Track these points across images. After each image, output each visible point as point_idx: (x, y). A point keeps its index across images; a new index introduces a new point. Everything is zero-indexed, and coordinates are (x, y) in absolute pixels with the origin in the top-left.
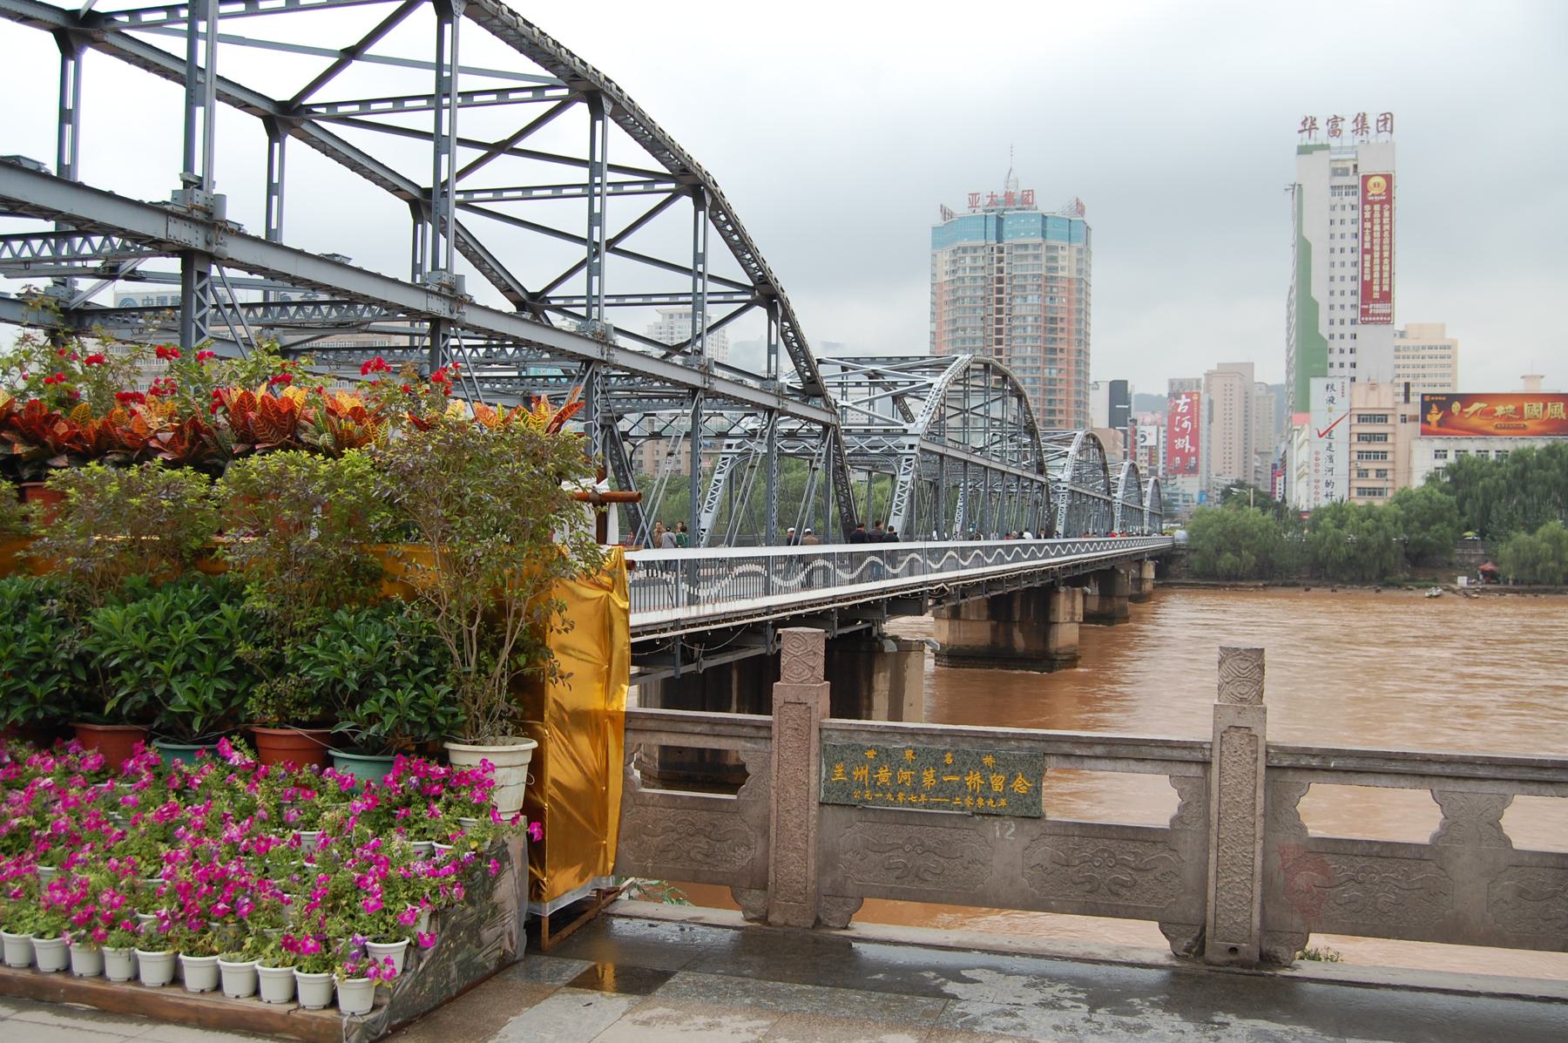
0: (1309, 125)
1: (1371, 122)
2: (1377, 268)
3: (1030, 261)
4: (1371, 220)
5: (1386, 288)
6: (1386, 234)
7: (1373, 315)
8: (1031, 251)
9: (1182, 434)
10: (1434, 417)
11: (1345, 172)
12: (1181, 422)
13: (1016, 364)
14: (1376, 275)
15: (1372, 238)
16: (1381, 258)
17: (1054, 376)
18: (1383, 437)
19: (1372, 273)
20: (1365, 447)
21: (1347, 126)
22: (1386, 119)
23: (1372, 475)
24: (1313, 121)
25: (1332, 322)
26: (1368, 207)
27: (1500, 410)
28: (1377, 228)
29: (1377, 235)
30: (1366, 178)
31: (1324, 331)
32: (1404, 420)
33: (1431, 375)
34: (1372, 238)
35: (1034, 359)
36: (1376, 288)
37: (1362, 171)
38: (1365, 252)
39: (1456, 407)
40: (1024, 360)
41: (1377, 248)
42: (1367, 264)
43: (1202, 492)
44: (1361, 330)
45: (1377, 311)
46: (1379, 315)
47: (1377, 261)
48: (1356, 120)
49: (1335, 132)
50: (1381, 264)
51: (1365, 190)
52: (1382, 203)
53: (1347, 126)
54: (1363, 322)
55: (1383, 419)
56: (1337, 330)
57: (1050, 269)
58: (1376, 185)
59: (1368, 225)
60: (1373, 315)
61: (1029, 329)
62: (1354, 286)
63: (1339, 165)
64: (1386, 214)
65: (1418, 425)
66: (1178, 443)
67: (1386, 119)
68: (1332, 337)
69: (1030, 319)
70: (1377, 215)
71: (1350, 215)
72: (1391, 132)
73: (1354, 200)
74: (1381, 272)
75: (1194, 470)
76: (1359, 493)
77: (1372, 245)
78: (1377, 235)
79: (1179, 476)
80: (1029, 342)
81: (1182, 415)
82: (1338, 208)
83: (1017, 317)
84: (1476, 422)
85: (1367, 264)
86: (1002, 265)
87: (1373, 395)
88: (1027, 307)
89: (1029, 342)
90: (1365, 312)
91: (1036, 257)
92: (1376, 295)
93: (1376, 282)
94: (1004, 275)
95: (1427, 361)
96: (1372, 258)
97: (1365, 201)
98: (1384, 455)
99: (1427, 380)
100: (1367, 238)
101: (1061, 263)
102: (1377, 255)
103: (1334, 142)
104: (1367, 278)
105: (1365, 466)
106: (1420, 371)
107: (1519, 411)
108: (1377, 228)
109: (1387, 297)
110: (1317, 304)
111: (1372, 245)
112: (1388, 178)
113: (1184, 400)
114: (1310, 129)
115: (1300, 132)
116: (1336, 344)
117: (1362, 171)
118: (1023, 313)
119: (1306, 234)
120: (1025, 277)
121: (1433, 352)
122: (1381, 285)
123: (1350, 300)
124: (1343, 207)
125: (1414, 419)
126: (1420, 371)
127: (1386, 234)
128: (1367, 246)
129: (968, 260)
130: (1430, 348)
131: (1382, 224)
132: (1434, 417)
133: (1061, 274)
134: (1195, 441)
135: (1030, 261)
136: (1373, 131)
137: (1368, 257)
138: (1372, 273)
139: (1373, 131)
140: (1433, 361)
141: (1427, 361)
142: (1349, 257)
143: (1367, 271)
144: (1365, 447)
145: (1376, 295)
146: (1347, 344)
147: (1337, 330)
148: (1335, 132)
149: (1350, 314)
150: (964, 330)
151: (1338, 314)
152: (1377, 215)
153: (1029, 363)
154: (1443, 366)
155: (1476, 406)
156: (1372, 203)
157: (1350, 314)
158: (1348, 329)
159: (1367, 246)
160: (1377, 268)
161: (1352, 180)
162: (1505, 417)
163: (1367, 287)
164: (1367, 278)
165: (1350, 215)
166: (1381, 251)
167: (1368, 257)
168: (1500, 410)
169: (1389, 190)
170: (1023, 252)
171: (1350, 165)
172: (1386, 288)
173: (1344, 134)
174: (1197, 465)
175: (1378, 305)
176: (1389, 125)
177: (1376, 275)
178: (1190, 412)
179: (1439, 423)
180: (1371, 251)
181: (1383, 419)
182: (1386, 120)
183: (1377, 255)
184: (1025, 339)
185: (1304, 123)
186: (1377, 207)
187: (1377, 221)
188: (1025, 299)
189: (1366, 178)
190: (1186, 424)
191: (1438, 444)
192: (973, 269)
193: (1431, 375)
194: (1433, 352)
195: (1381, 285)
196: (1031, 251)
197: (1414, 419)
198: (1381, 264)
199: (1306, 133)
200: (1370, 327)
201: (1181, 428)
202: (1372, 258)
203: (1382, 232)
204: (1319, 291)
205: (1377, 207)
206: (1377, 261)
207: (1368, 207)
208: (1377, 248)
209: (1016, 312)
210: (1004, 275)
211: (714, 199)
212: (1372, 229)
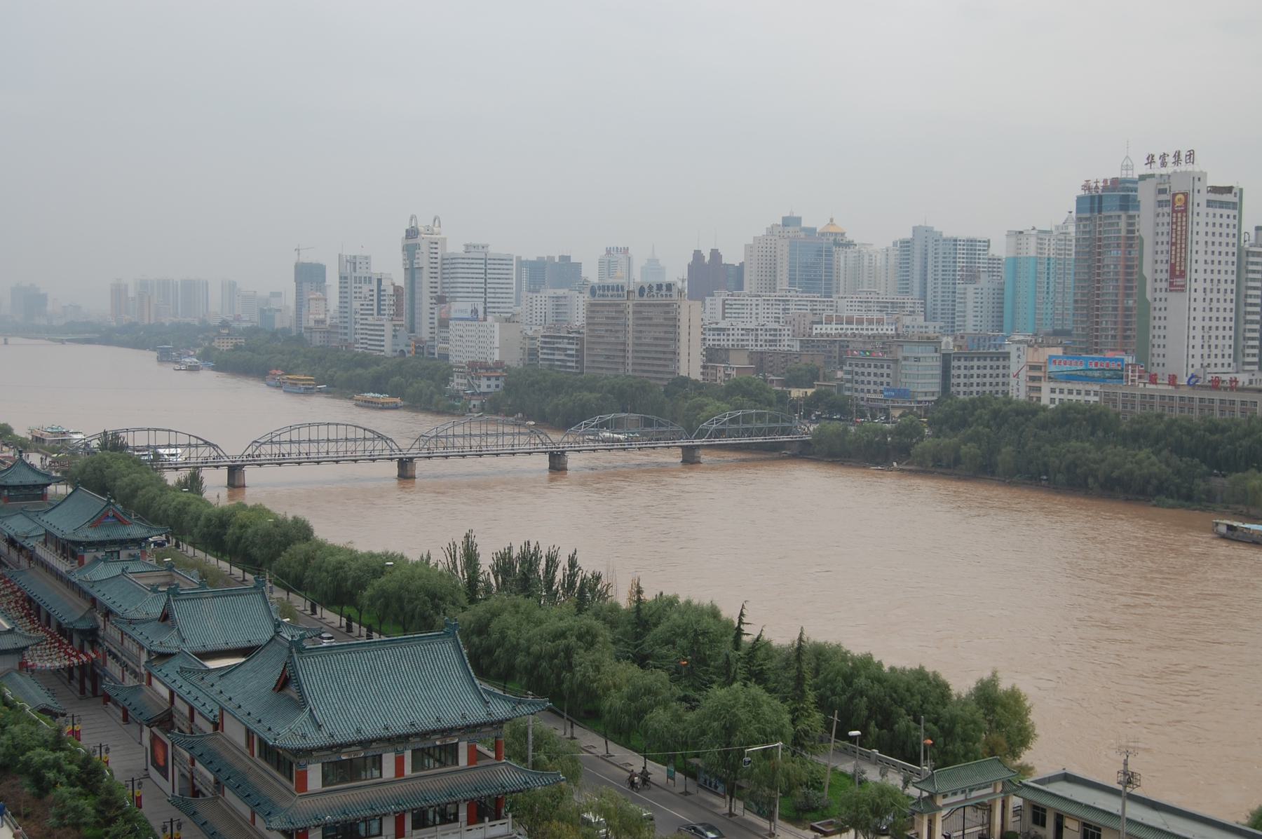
1: (1183, 157)
2: (1178, 255)
4: (1176, 223)
5: (1183, 268)
6: (1184, 232)
7: (1176, 286)
14: (1178, 260)
15: (1176, 234)
16: (1181, 248)
19: (1176, 258)
21: (1170, 160)
24: (1153, 156)
26: (1174, 215)
28: (1179, 228)
29: (1179, 233)
30: (1175, 195)
31: (1149, 296)
34: (1176, 234)
36: (1178, 268)
38: (1173, 244)
41: (1179, 242)
42: (1173, 253)
45: (1178, 284)
46: (1178, 286)
47: (1178, 250)
48: (1175, 155)
50: (1181, 252)
51: (1174, 204)
52: (1182, 211)
53: (1170, 160)
54: (1171, 291)
56: (1158, 295)
58: (1180, 200)
59: (1174, 227)
60: (1176, 286)
62: (1166, 267)
64: (1184, 219)
69: (1112, 267)
70: (1179, 220)
71: (1167, 219)
72: (1193, 163)
73: (1167, 210)
74: (1181, 257)
77: (1176, 240)
78: (1179, 233)
85: (1173, 253)
88: (1113, 256)
90: (1171, 284)
92: (1178, 273)
93: (1178, 264)
96: (1176, 248)
97: (1174, 211)
100: (1174, 235)
102: (1178, 246)
104: (1173, 261)
108: (1179, 228)
109: (1183, 274)
110: (1146, 279)
111: (1176, 240)
114: (1151, 162)
122: (1180, 266)
123: (1165, 276)
124: (1163, 215)
127: (1184, 232)
128: (1174, 240)
131: (1182, 226)
137: (1174, 248)
138: (1176, 258)
142: (1165, 247)
143: (1173, 257)
145: (1178, 273)
147: (1158, 295)
148: (1164, 164)
149: (1165, 285)
151: (1158, 285)
152: (1179, 220)
156: (1177, 212)
158: (1163, 295)
159: (1174, 240)
160: (1178, 255)
163: (1173, 267)
164: (1173, 261)
166: (1181, 243)
167: (1174, 248)
169: (1186, 203)
172: (1183, 268)
173: (1168, 165)
175: (1178, 280)
177: (1178, 260)
182: (1191, 154)
183: (1178, 246)
185: (1148, 159)
186: (1179, 215)
187: (1179, 224)
189: (1175, 195)
195: (1180, 266)
198: (1181, 252)
200: (1174, 294)
202: (1176, 248)
203: (1182, 231)
205: (1179, 215)
206: (1178, 250)
207: (1174, 215)
208: (1179, 242)
212: (1176, 229)
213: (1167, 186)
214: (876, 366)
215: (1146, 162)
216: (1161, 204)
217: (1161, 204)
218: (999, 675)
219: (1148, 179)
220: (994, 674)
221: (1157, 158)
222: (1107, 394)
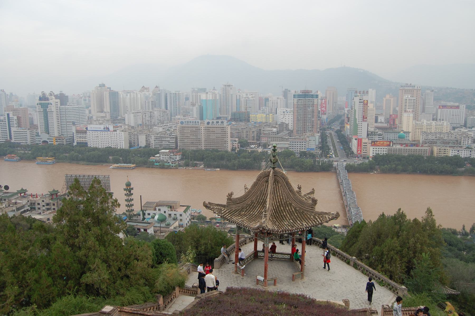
1: (365, 92)
3: (310, 102)
8: (310, 100)
9: (323, 107)
10: (373, 144)
11: (361, 100)
12: (323, 105)
13: (308, 118)
18: (366, 146)
20: (364, 147)
27: (381, 143)
30: (364, 101)
31: (357, 122)
32: (369, 143)
35: (311, 118)
37: (364, 99)
39: (376, 142)
40: (309, 118)
43: (327, 118)
44: (362, 122)
51: (364, 103)
55: (366, 143)
56: (359, 122)
57: (313, 103)
62: (362, 116)
65: (370, 144)
66: (323, 109)
71: (362, 106)
75: (325, 114)
80: (310, 115)
81: (323, 103)
84: (378, 144)
89: (310, 115)
90: (363, 120)
91: (311, 101)
95: (370, 111)
97: (364, 104)
98: (366, 148)
99: (370, 114)
101: (315, 102)
105: (364, 149)
107: (384, 143)
109: (366, 118)
112: (367, 101)
113: (324, 100)
116: (359, 124)
117: (364, 99)
119: (355, 108)
121: (371, 110)
123: (362, 118)
125: (370, 143)
129: (300, 102)
132: (373, 144)
133: (315, 104)
134: (326, 109)
135: (310, 102)
136: (365, 93)
139: (365, 93)
141: (370, 111)
144: (364, 147)
146: (361, 124)
149: (361, 120)
151: (359, 120)
153: (310, 118)
155: (378, 142)
157: (361, 120)
158: (361, 122)
161: (362, 101)
162: (382, 144)
163: (364, 116)
165: (362, 106)
168: (381, 143)
170: (309, 100)
171: (362, 99)
174: (326, 113)
179: (374, 144)
180: (364, 111)
181: (366, 143)
188: (309, 108)
189: (364, 101)
190: (324, 105)
191: (373, 147)
192: (301, 103)
194: (371, 110)
196: (310, 100)
197: (370, 143)
204: (357, 117)
213: (362, 99)
214: (300, 142)
216: (360, 102)
217: (360, 102)
218: (384, 213)
220: (383, 212)
222: (389, 149)
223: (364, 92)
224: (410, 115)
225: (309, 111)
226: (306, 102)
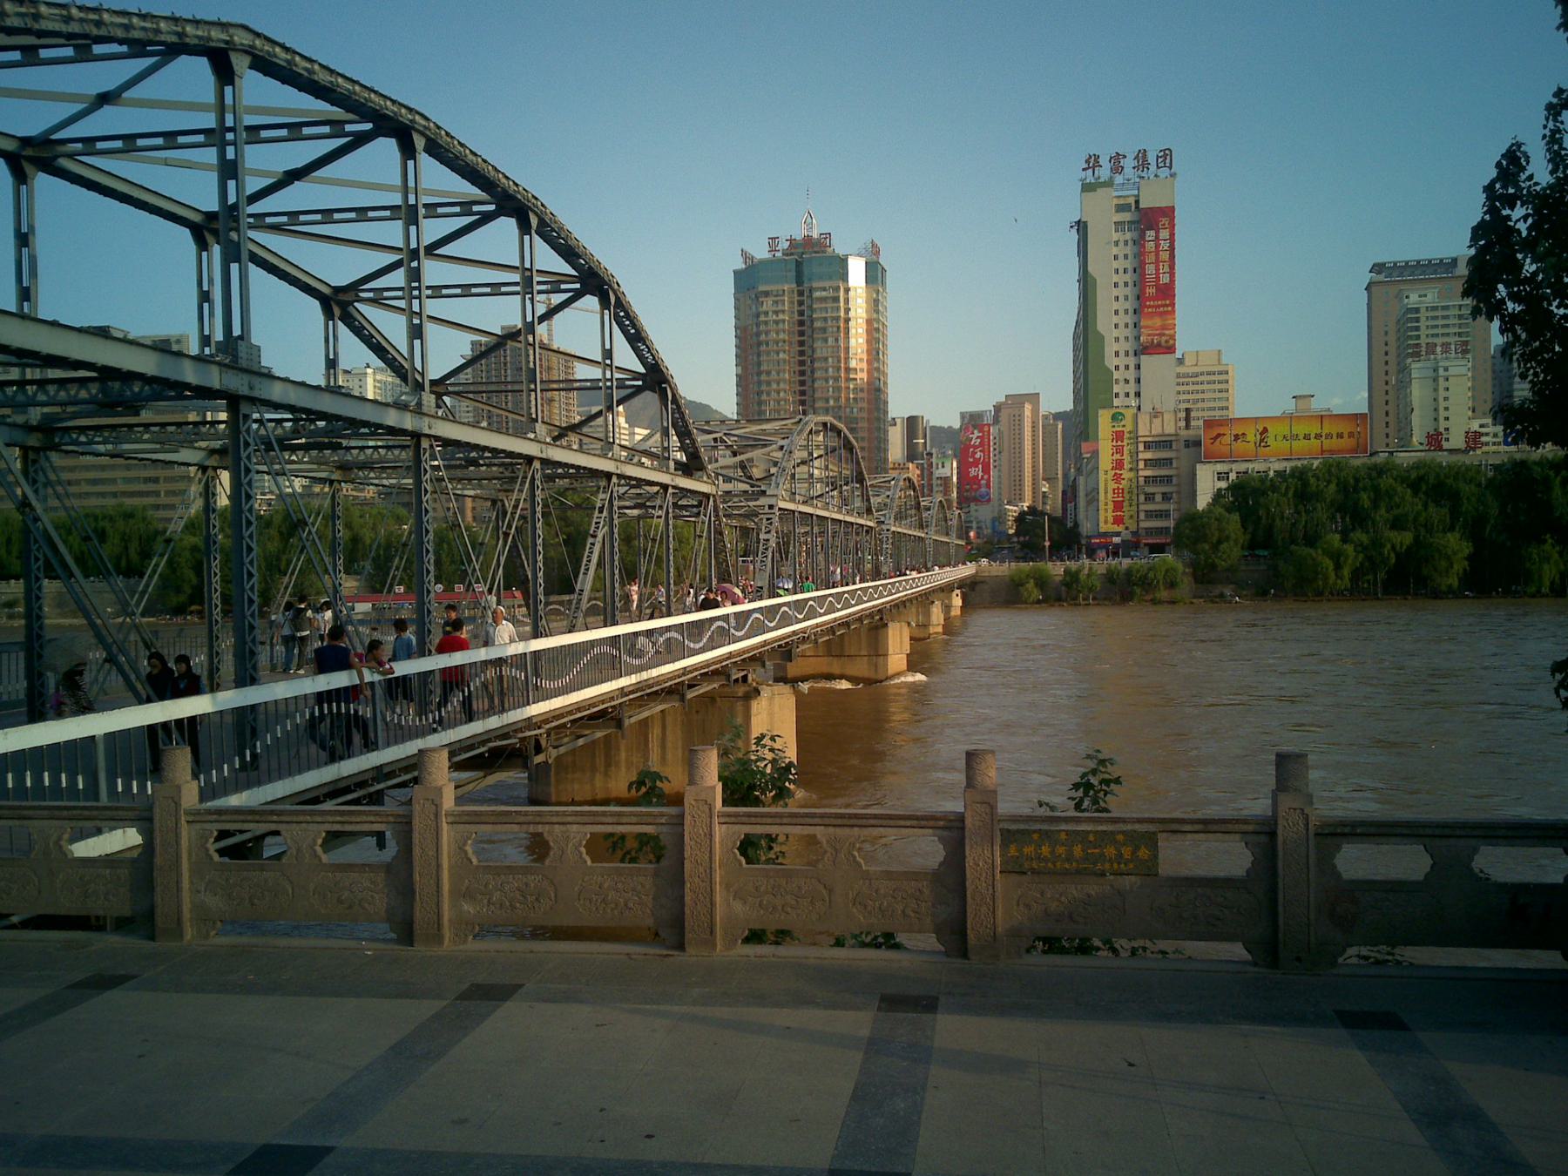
0: (1093, 162)
1: (1151, 158)
17: (855, 415)
21: (1128, 163)
22: (1165, 155)
23: (1158, 498)
24: (1097, 160)
25: (1117, 354)
33: (1209, 400)
48: (1136, 158)
49: (1117, 169)
53: (1128, 163)
61: (830, 370)
63: (1122, 201)
67: (1165, 155)
68: (1117, 368)
72: (1170, 168)
76: (1146, 516)
79: (972, 505)
81: (975, 447)
82: (1121, 244)
83: (819, 359)
86: (802, 308)
87: (1157, 421)
94: (805, 318)
95: (1205, 387)
99: (1205, 405)
103: (1119, 179)
105: (1150, 490)
106: (1200, 396)
115: (1084, 170)
118: (825, 355)
120: (825, 319)
126: (1200, 396)
130: (1209, 374)
134: (986, 470)
136: (1153, 168)
139: (1153, 168)
140: (1211, 387)
141: (1205, 387)
148: (1117, 169)
150: (768, 373)
154: (1220, 391)
171: (1132, 201)
176: (1168, 161)
178: (982, 444)
184: (827, 381)
185: (1087, 161)
188: (826, 340)
190: (977, 456)
193: (1209, 400)
199: (1091, 170)
201: (974, 458)
209: (818, 354)
210: (805, 318)
211: (618, 299)
215: (1086, 166)
219: (1098, 190)
221: (1104, 161)
223: (1142, 159)
224: (1452, 371)
225: (826, 359)
226: (803, 308)
